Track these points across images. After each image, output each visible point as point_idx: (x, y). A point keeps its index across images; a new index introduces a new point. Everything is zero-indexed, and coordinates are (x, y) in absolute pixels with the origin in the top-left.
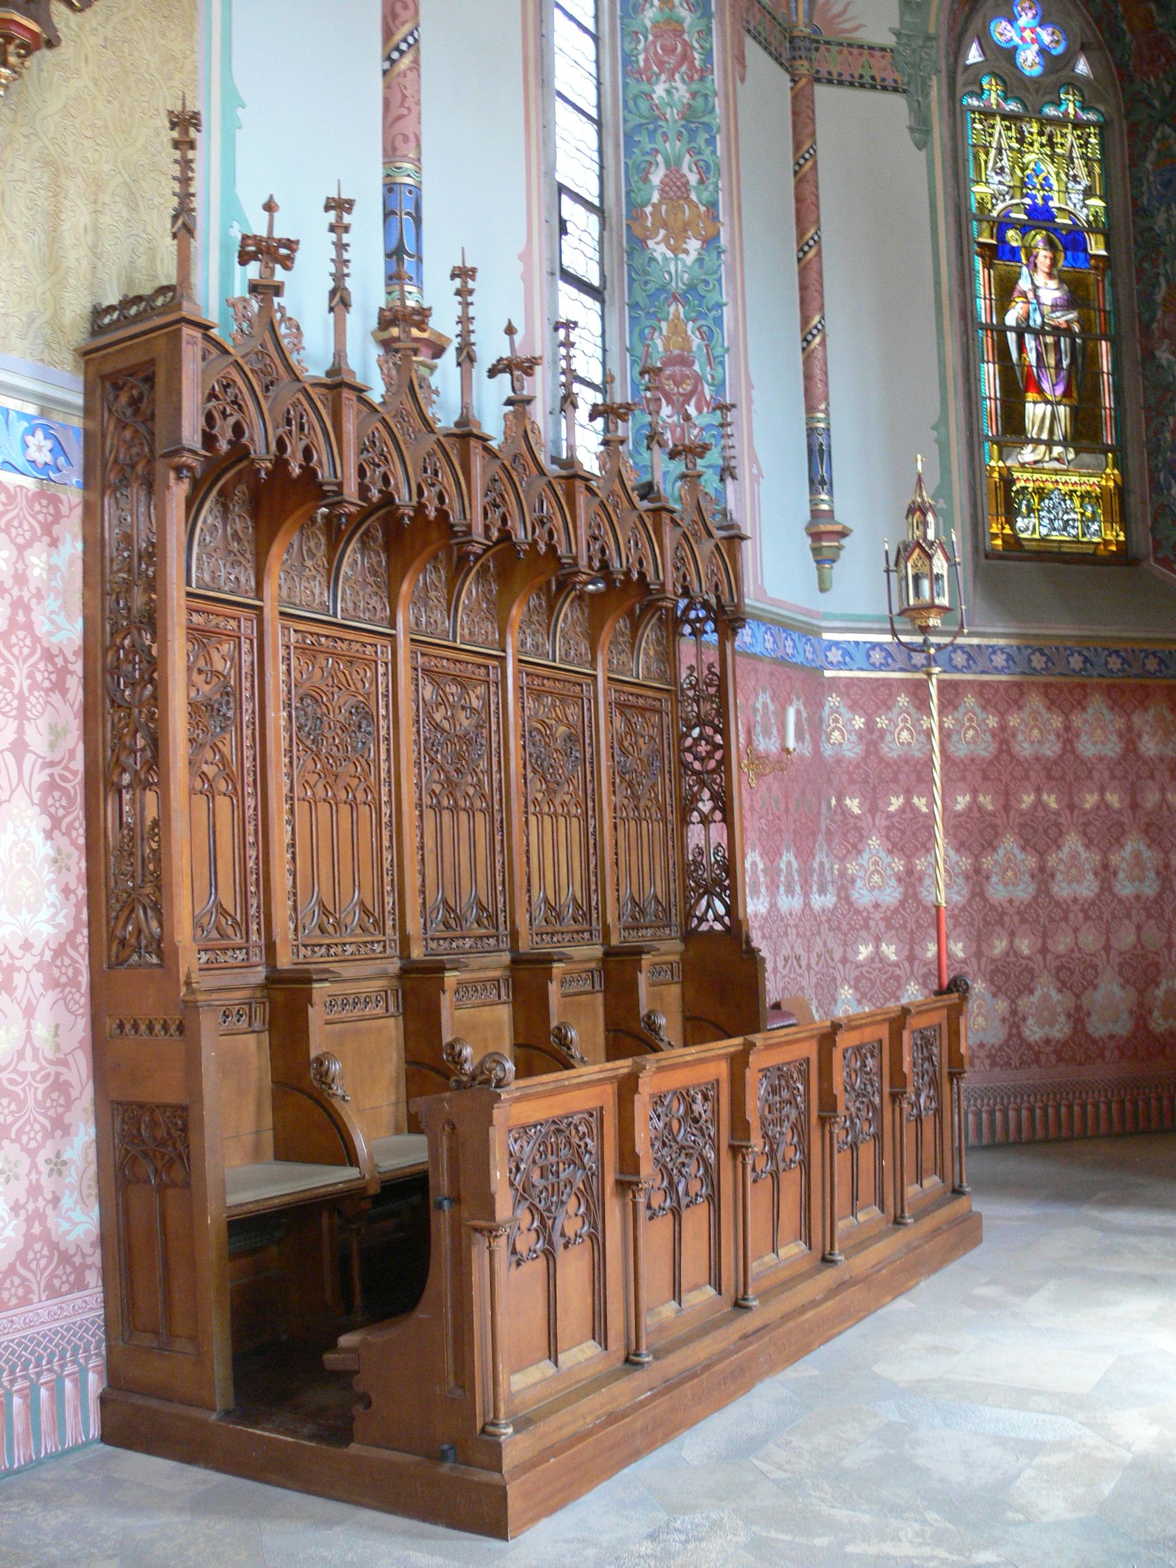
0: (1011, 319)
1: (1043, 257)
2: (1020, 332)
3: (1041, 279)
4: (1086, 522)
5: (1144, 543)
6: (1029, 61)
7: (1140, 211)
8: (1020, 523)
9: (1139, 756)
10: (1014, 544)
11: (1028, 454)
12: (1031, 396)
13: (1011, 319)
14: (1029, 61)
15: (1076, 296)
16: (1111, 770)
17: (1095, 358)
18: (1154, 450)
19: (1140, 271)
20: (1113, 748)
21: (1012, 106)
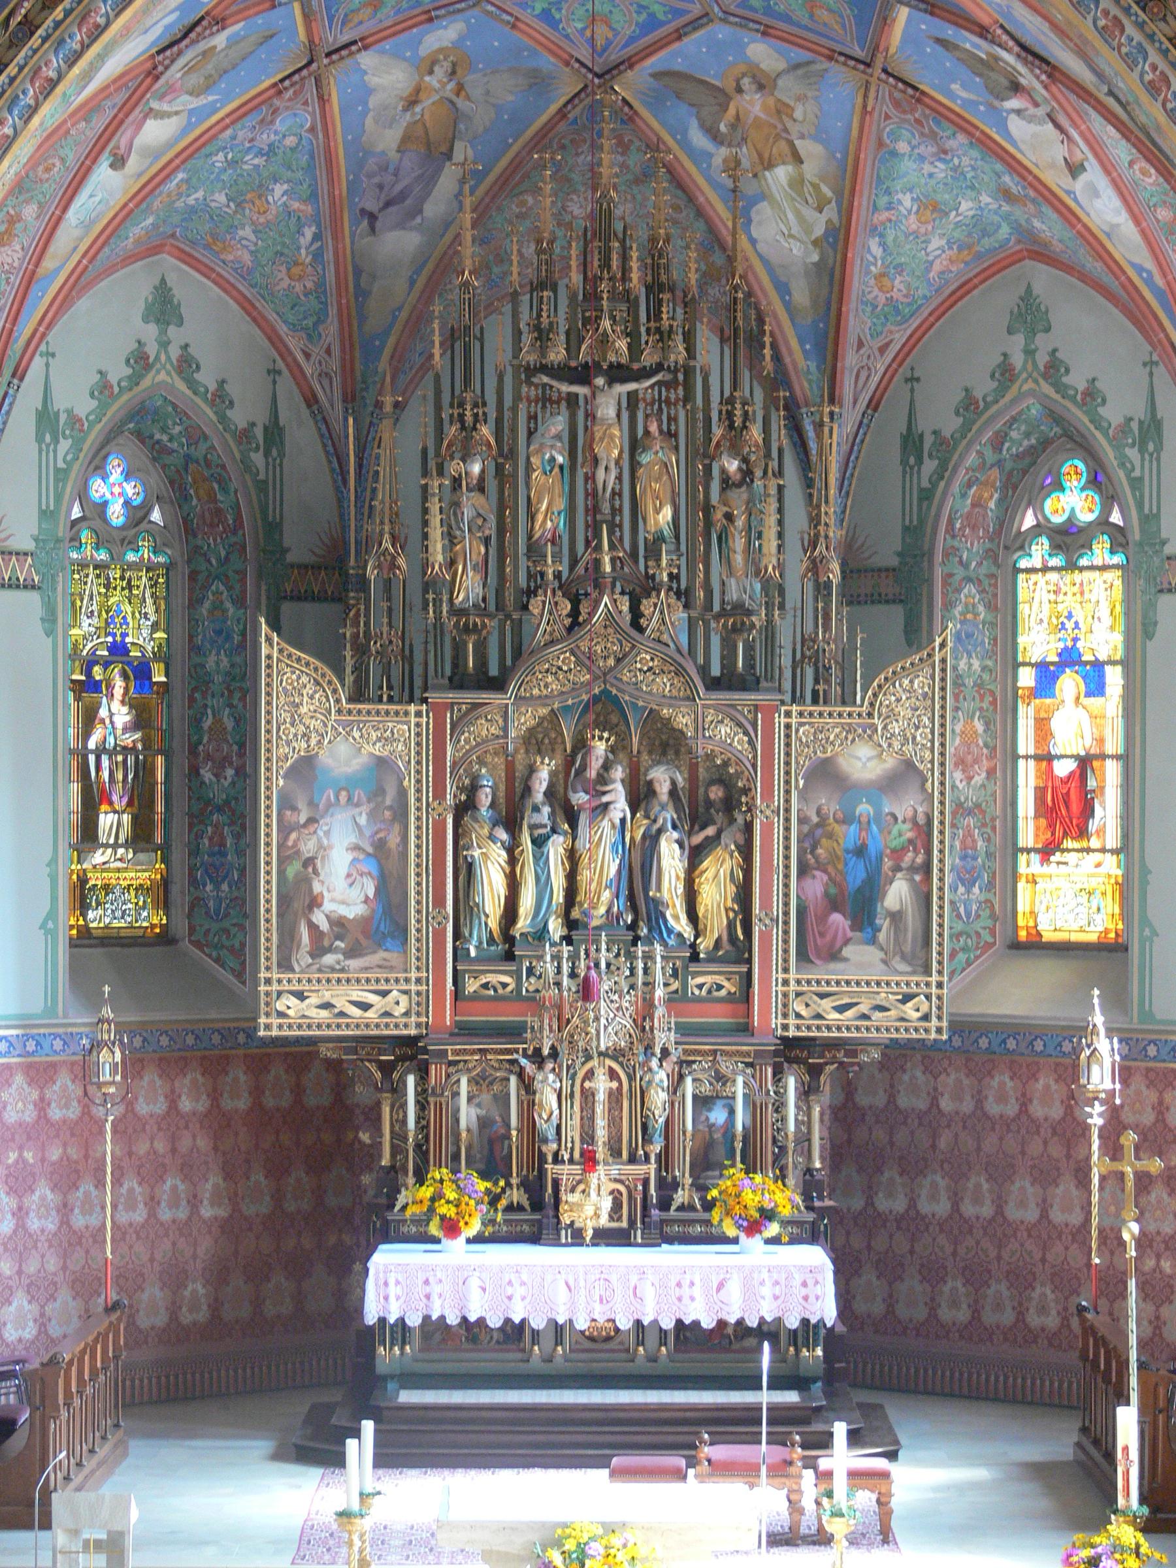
0: (92, 745)
1: (119, 685)
3: (116, 706)
4: (139, 909)
5: (181, 927)
6: (116, 514)
7: (195, 649)
8: (91, 915)
9: (178, 1112)
11: (99, 857)
12: (104, 808)
13: (92, 745)
14: (116, 514)
15: (140, 721)
16: (159, 1124)
17: (152, 771)
18: (194, 852)
19: (192, 700)
20: (160, 1107)
21: (102, 556)
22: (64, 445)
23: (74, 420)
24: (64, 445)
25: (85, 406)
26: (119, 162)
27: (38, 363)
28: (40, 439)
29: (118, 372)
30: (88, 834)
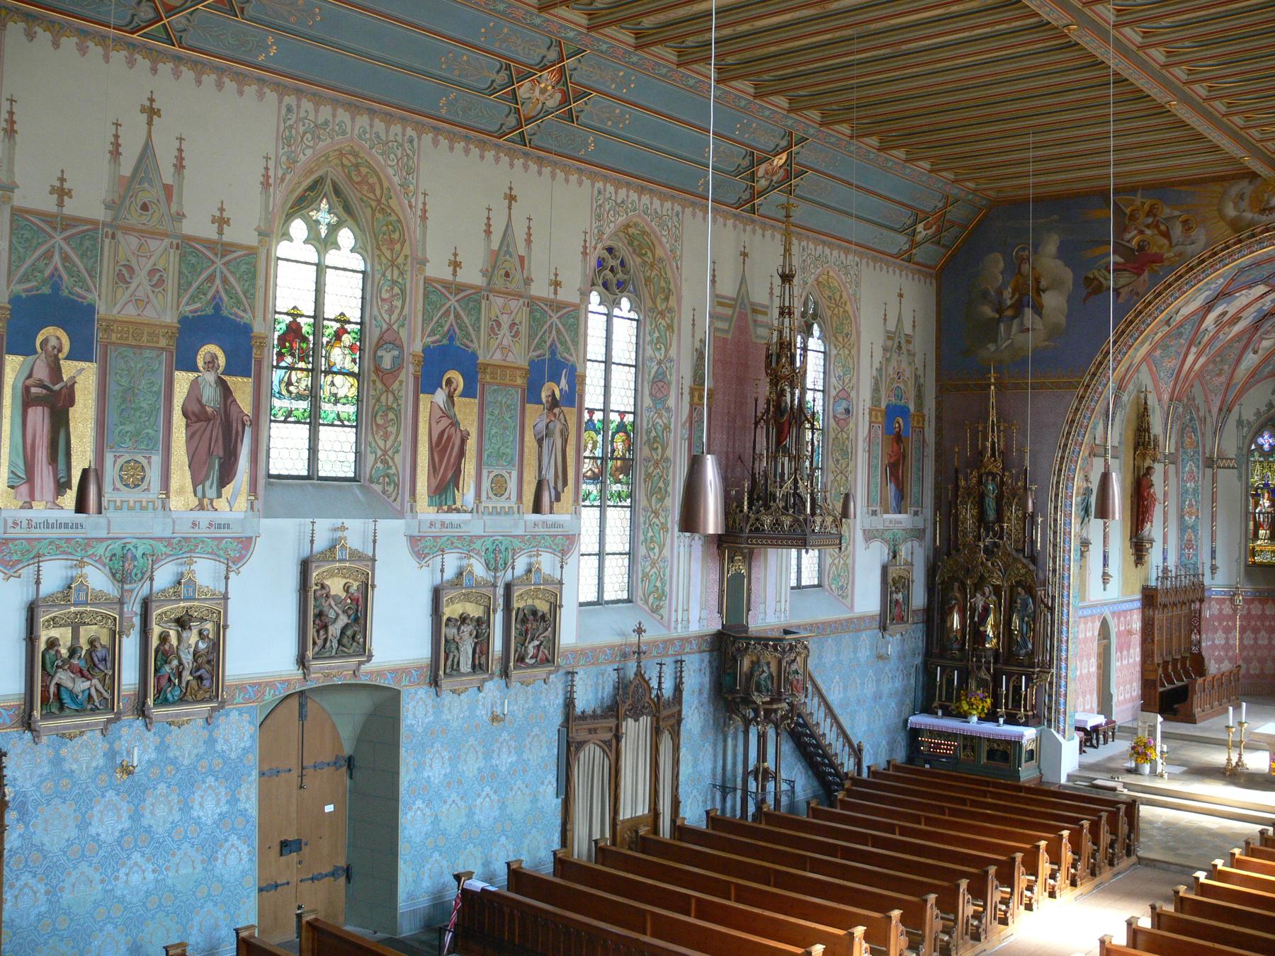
2: (1259, 513)
6: (1266, 447)
10: (1254, 563)
11: (1259, 542)
14: (1266, 447)
21: (1262, 459)
22: (1245, 429)
23: (1249, 423)
24: (1245, 429)
25: (1252, 418)
26: (1255, 352)
27: (1236, 408)
28: (1237, 427)
29: (1263, 409)
30: (1256, 536)
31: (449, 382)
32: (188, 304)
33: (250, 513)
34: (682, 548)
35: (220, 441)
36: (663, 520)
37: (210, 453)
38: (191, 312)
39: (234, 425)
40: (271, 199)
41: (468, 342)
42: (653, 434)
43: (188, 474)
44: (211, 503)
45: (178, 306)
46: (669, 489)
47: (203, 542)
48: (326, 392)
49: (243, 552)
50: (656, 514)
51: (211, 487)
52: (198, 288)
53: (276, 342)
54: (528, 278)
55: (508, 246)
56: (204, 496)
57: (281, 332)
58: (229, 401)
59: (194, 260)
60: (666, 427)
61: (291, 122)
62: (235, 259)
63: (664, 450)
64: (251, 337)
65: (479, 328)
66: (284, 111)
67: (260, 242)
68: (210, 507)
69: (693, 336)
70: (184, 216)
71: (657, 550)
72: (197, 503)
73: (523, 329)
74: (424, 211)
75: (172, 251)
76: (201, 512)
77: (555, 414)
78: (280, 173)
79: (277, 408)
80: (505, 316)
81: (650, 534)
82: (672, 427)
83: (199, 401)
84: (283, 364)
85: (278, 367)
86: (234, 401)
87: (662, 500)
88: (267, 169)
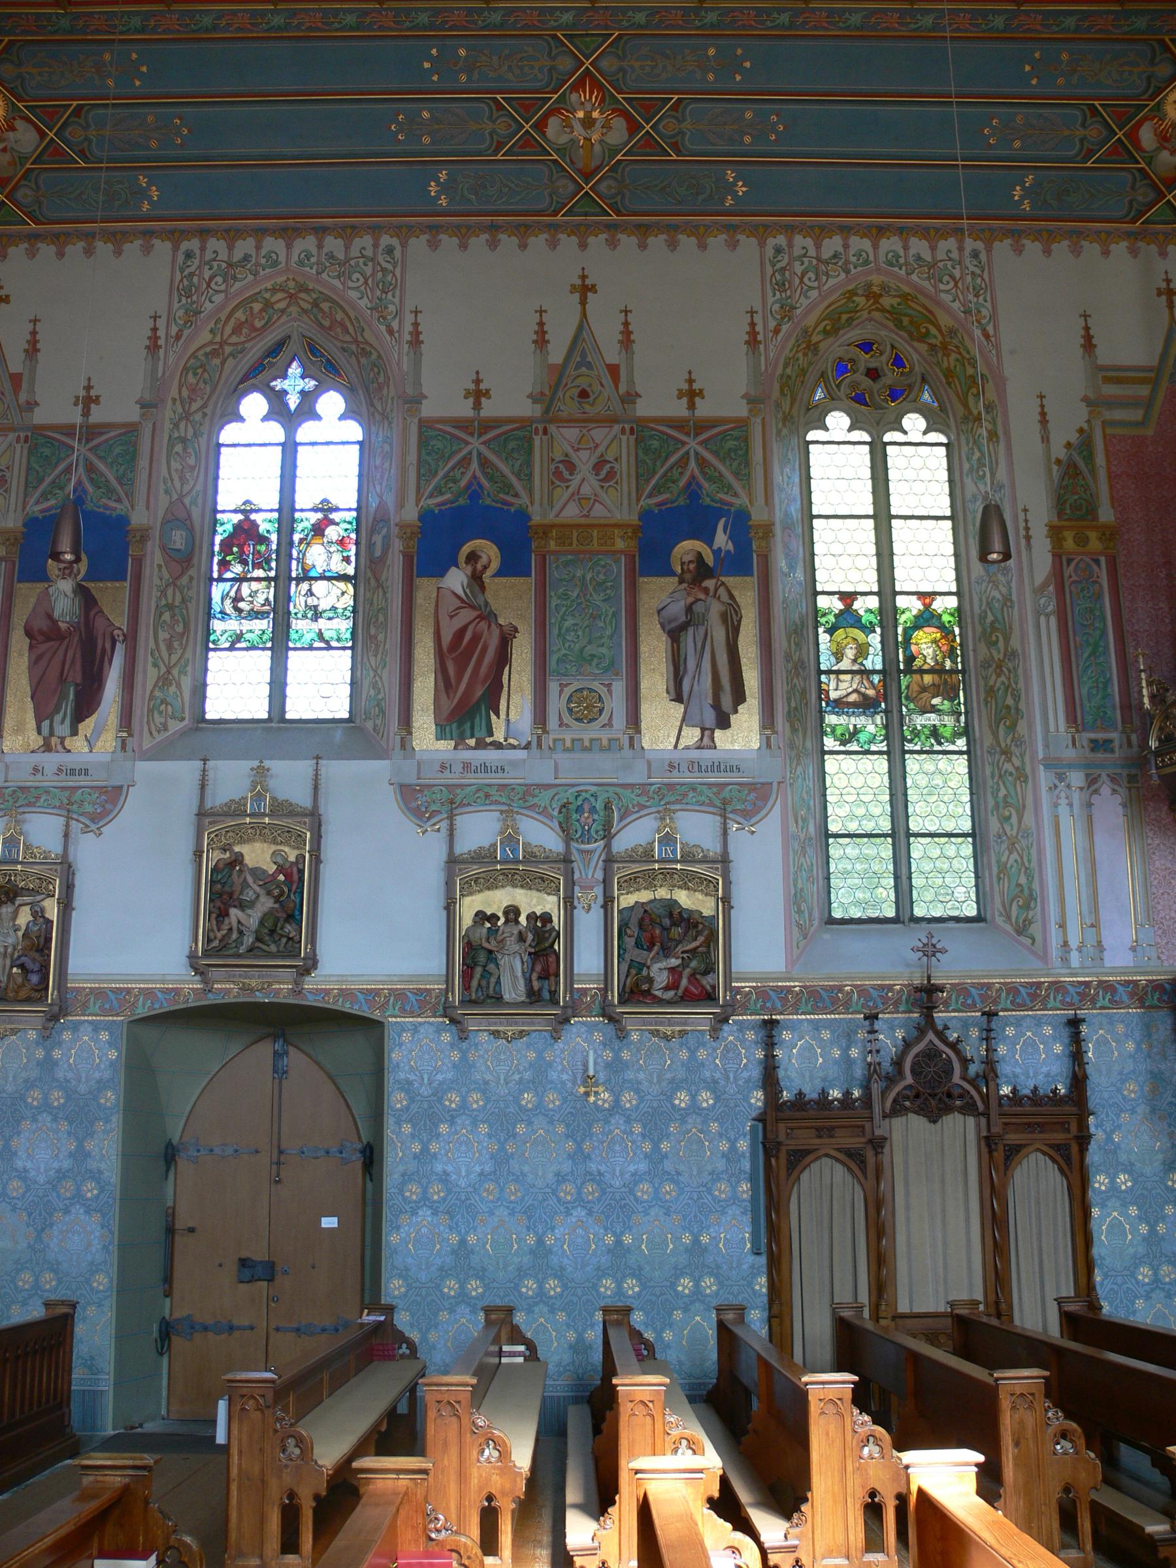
31: (473, 557)
32: (37, 503)
33: (120, 754)
34: (1063, 810)
35: (78, 667)
36: (1017, 763)
37: (62, 679)
38: (42, 511)
39: (100, 642)
40: (161, 363)
41: (509, 498)
42: (990, 618)
43: (30, 706)
44: (62, 743)
45: (24, 508)
46: (1022, 706)
47: (47, 792)
48: (298, 603)
49: (108, 806)
50: (1007, 753)
51: (62, 722)
52: (53, 482)
53: (217, 548)
54: (628, 394)
55: (583, 354)
56: (52, 734)
57: (225, 535)
58: (92, 613)
59: (47, 451)
60: (1007, 601)
61: (192, 269)
62: (106, 441)
63: (1007, 639)
64: (128, 532)
65: (530, 476)
66: (181, 258)
67: (143, 415)
68: (59, 747)
69: (1046, 439)
70: (37, 404)
71: (1014, 820)
72: (41, 742)
73: (625, 467)
74: (416, 333)
75: (18, 446)
76: (47, 754)
77: (706, 591)
78: (174, 330)
79: (218, 633)
80: (584, 454)
81: (1003, 792)
82: (1014, 598)
83: (50, 617)
84: (228, 575)
85: (221, 579)
86: (101, 611)
87: (1013, 727)
88: (155, 329)
